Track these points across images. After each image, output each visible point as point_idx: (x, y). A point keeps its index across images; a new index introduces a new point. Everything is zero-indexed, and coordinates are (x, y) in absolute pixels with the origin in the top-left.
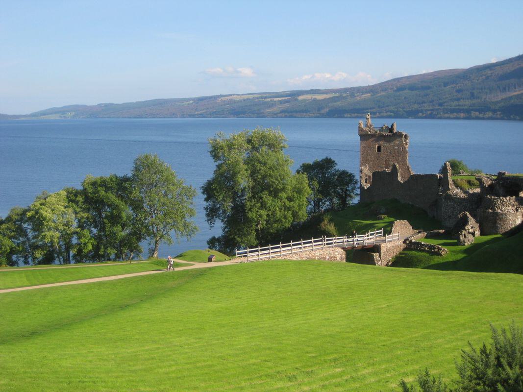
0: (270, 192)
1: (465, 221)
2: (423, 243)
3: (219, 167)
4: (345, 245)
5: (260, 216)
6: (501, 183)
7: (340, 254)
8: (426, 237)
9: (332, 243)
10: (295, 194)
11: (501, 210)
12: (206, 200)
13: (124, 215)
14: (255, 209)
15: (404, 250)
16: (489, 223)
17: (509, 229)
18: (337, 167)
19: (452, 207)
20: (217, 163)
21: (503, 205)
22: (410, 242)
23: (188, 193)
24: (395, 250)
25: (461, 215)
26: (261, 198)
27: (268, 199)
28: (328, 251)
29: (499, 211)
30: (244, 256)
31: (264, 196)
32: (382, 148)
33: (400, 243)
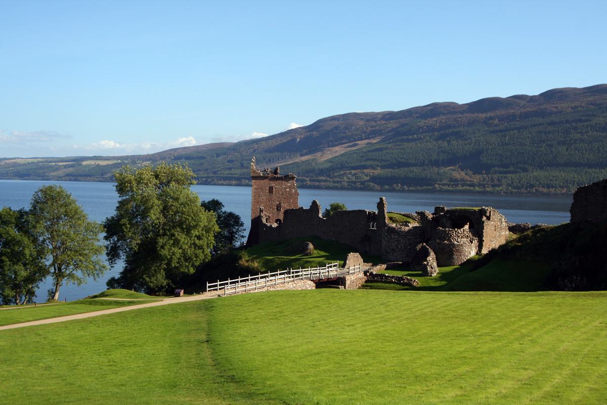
0: (182, 229)
1: (428, 254)
2: (387, 275)
3: (122, 204)
4: (314, 277)
5: (174, 254)
6: (448, 216)
7: (310, 285)
8: (386, 269)
9: (298, 276)
10: (204, 233)
11: (458, 242)
12: (106, 238)
13: (27, 252)
14: (167, 247)
15: (366, 282)
16: (446, 254)
17: (465, 260)
18: (223, 210)
19: (397, 241)
20: (120, 199)
21: (459, 237)
22: (371, 274)
23: (89, 228)
24: (358, 283)
25: (419, 247)
26: (174, 235)
27: (182, 238)
28: (300, 284)
29: (456, 243)
30: (214, 290)
31: (176, 233)
32: (274, 190)
33: (361, 275)
